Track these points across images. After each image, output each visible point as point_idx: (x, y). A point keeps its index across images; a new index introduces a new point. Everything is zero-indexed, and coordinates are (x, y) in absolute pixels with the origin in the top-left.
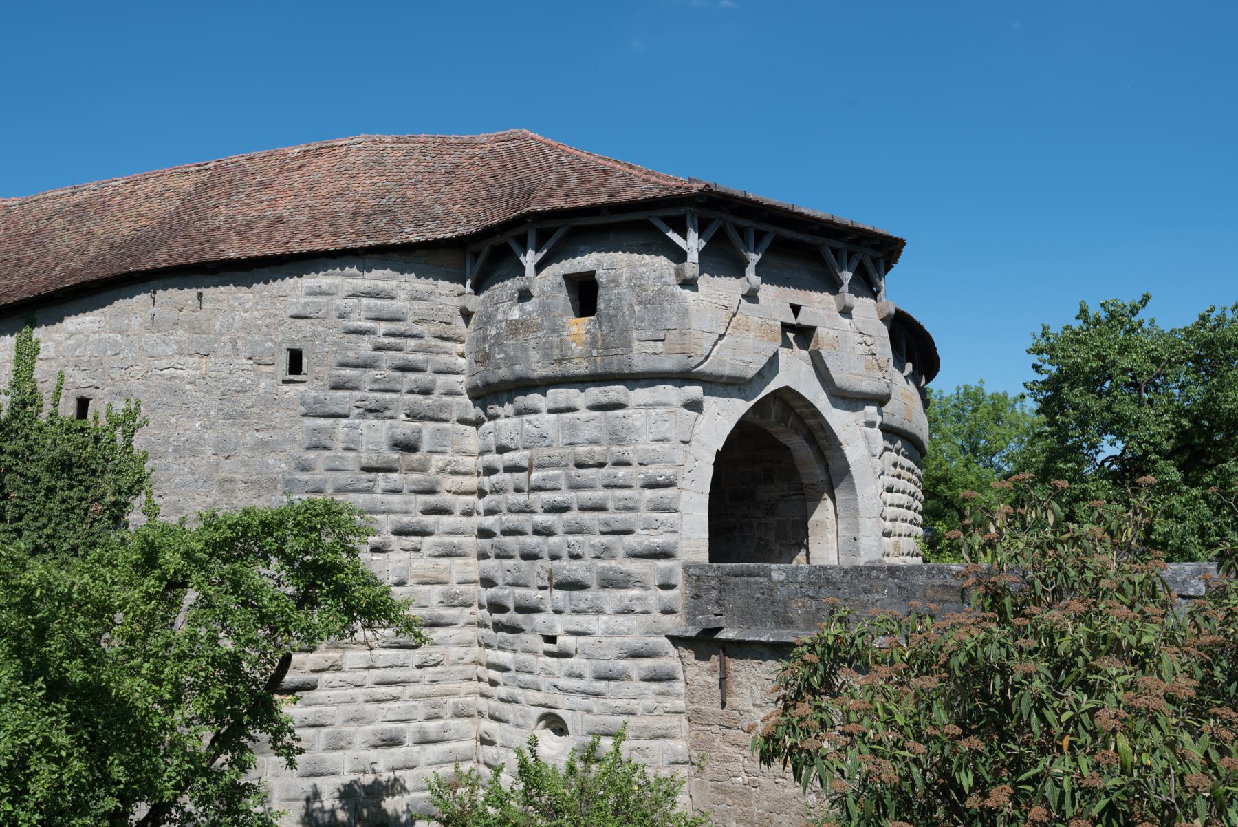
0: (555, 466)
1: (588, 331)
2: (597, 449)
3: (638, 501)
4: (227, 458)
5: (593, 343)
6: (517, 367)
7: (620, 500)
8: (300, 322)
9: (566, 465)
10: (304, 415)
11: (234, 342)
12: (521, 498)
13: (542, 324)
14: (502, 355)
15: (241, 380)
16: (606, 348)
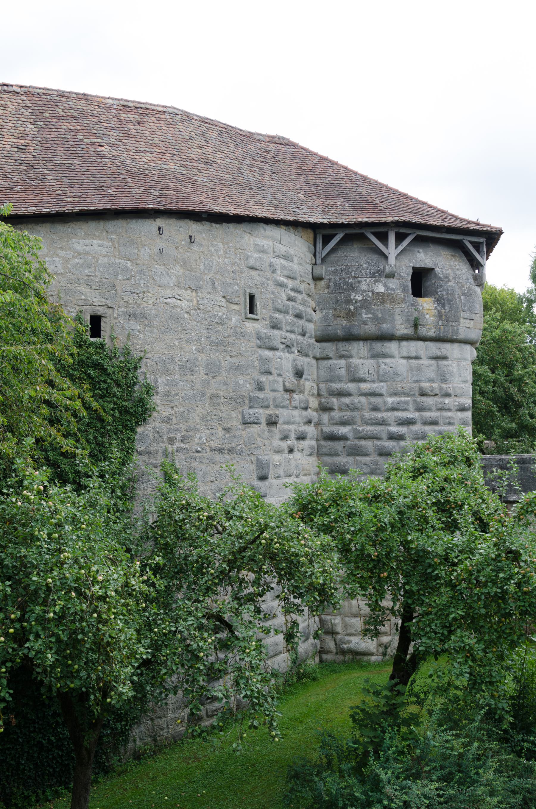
0: (407, 394)
1: (436, 308)
2: (433, 385)
3: (454, 419)
4: (213, 378)
5: (440, 316)
6: (384, 326)
7: (447, 418)
8: (253, 273)
9: (414, 395)
10: (259, 347)
11: (213, 281)
12: (379, 415)
13: (404, 299)
14: (370, 316)
15: (220, 314)
16: (447, 321)
